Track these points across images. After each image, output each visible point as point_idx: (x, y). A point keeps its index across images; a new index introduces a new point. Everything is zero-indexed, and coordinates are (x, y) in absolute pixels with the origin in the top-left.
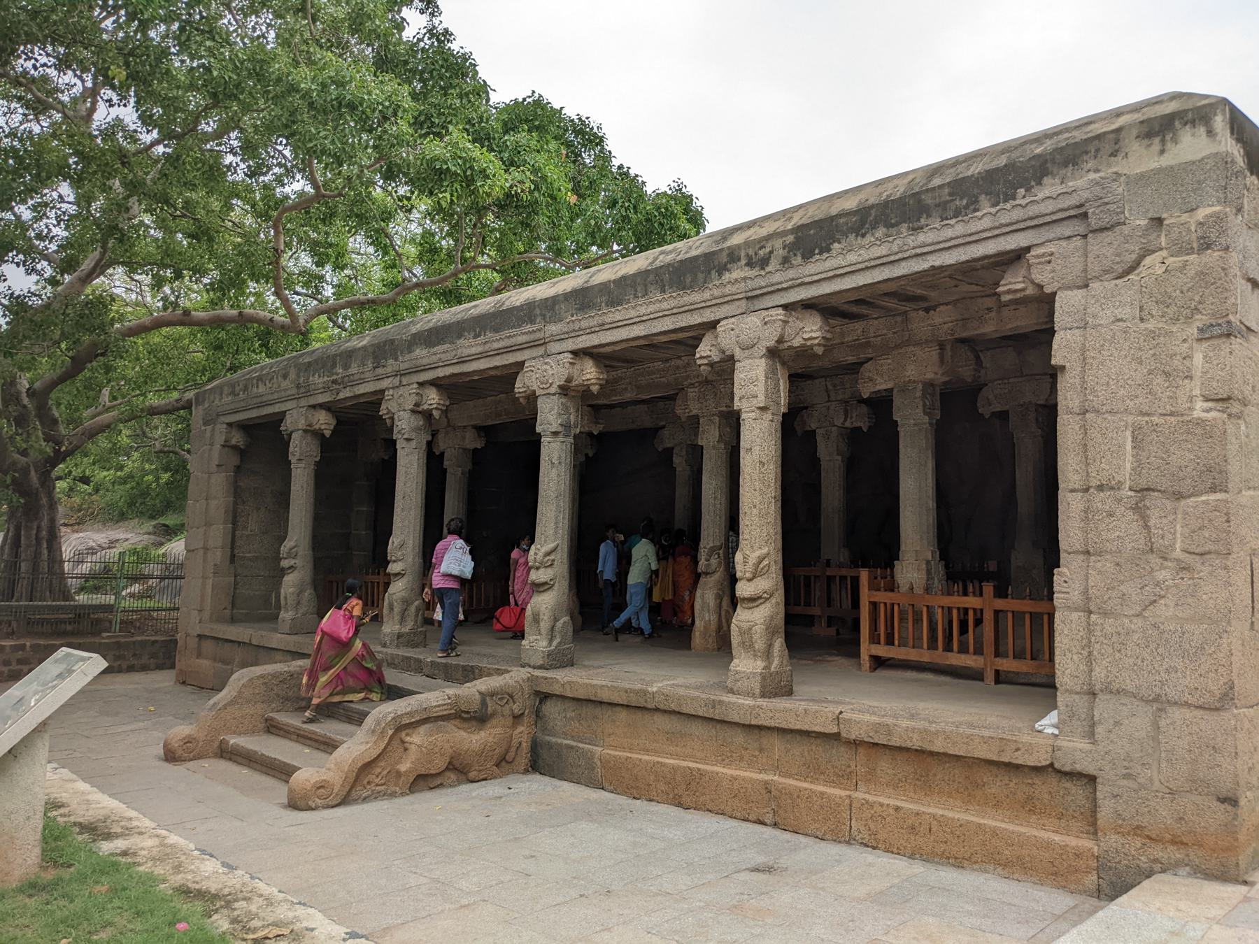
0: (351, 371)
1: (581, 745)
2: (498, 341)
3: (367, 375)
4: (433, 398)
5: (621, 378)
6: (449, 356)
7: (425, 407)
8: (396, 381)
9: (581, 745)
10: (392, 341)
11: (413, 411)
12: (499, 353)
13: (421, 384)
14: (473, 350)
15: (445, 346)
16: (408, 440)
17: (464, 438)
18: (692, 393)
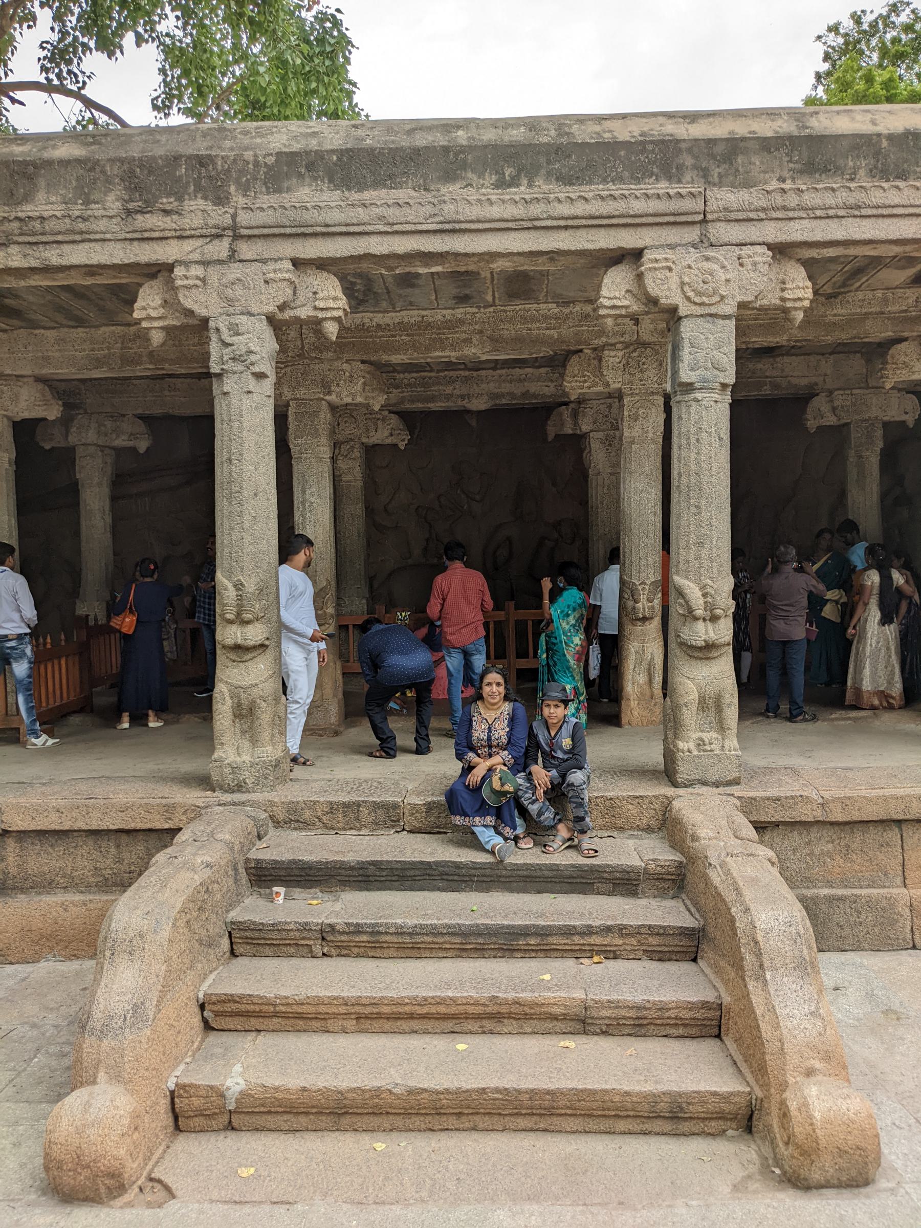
0: (27, 210)
1: (857, 892)
2: (589, 199)
3: (102, 225)
4: (327, 298)
5: (461, 322)
6: (411, 214)
7: (304, 313)
8: (221, 249)
9: (857, 892)
10: (202, 161)
11: (271, 319)
12: (569, 225)
13: (297, 263)
14: (495, 212)
15: (401, 194)
16: (260, 376)
17: (16, 398)
18: (613, 358)
